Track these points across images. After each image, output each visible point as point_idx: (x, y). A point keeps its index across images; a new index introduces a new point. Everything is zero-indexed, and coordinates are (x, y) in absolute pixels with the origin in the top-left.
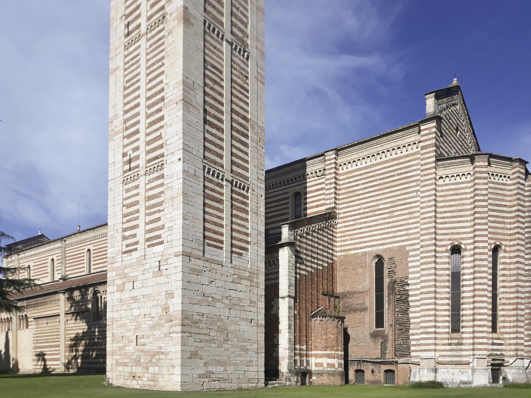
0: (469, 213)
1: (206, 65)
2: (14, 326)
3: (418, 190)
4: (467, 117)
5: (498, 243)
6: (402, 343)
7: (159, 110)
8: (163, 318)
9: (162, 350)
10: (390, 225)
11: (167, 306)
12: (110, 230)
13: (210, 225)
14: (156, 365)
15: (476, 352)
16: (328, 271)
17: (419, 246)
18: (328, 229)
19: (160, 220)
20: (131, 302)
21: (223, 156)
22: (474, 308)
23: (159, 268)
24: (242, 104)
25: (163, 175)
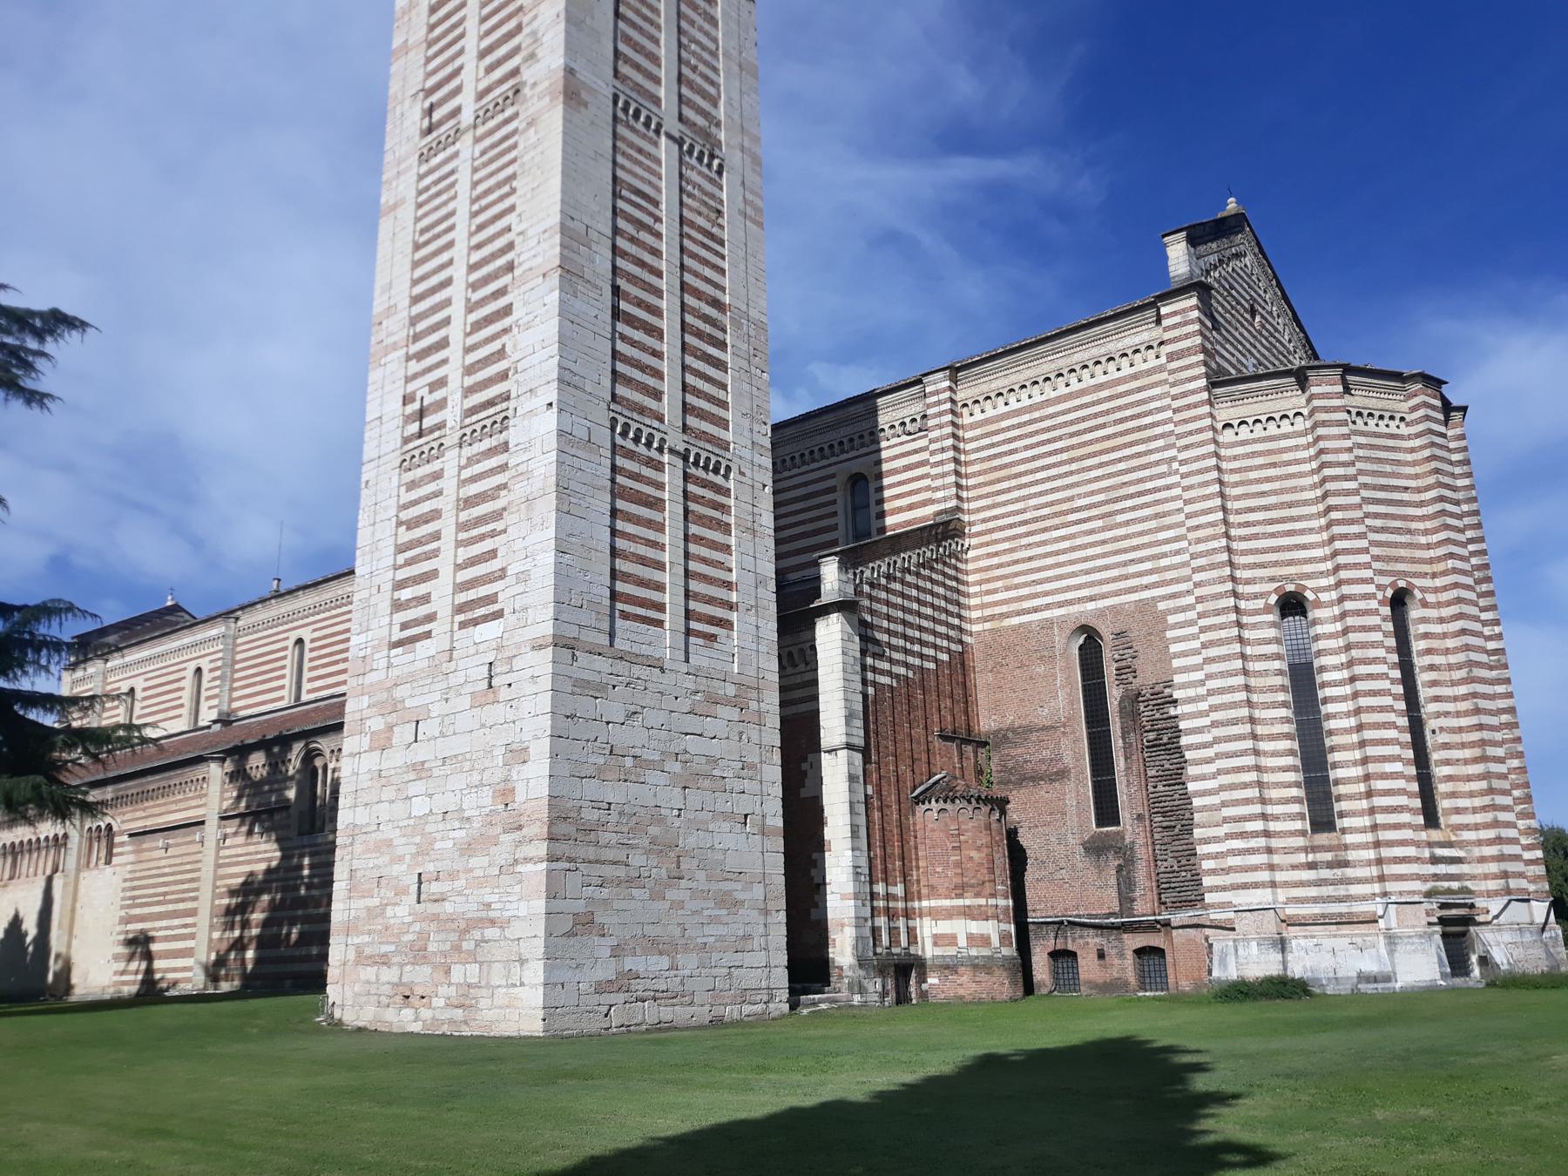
0: (1313, 509)
1: (618, 188)
2: (71, 859)
3: (1173, 459)
4: (1274, 282)
5: (1402, 584)
6: (1176, 868)
7: (502, 292)
8: (496, 819)
9: (492, 914)
11: (510, 786)
12: (359, 588)
13: (628, 563)
14: (472, 958)
15: (1390, 886)
16: (951, 675)
17: (1190, 600)
18: (945, 563)
19: (495, 557)
20: (406, 779)
21: (661, 393)
22: (1365, 761)
23: (490, 683)
24: (708, 272)
25: (506, 443)
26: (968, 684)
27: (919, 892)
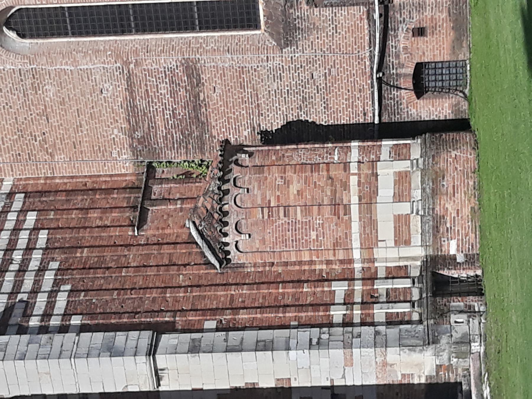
16: (56, 210)
26: (69, 187)
27: (342, 262)
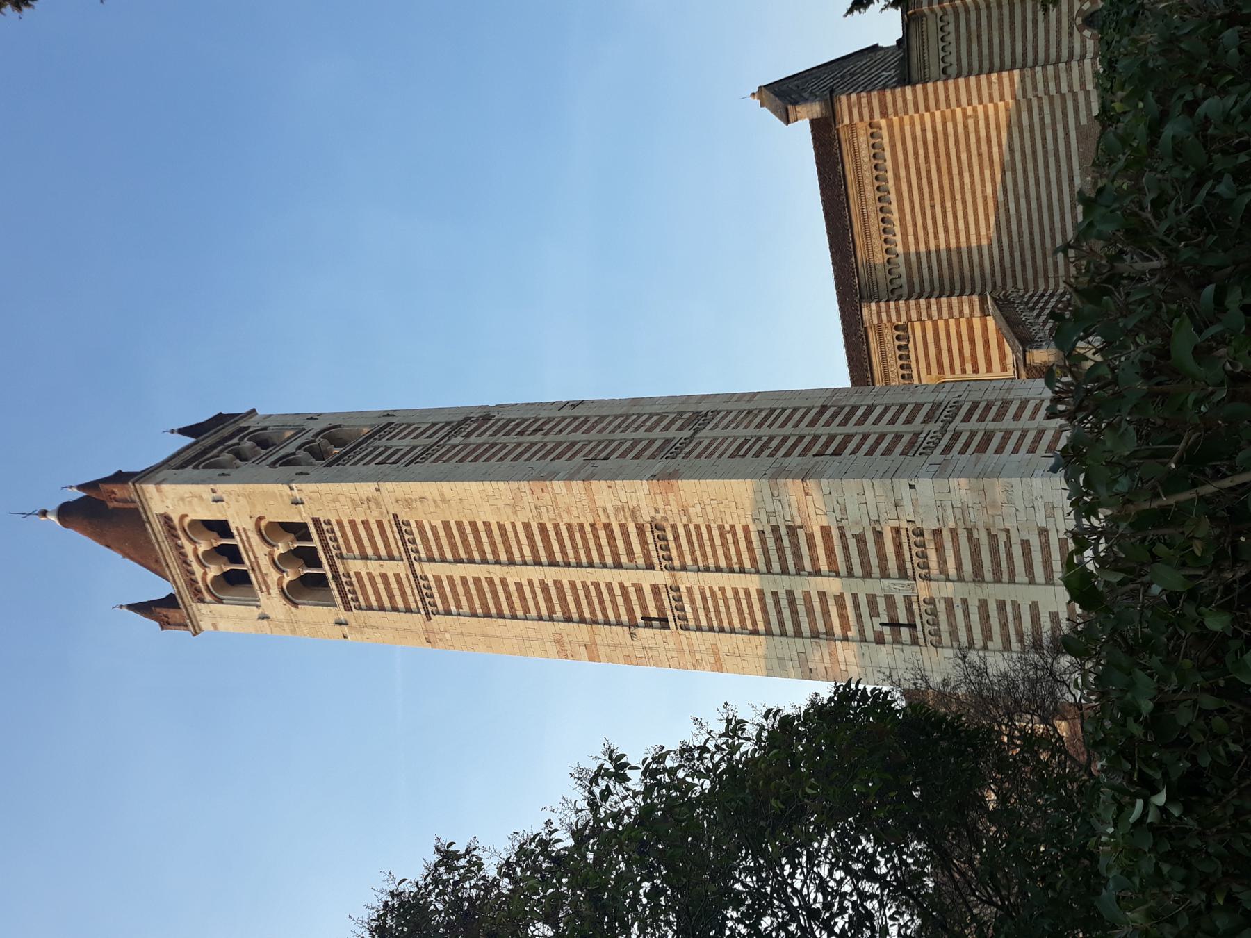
10: (1030, 166)
